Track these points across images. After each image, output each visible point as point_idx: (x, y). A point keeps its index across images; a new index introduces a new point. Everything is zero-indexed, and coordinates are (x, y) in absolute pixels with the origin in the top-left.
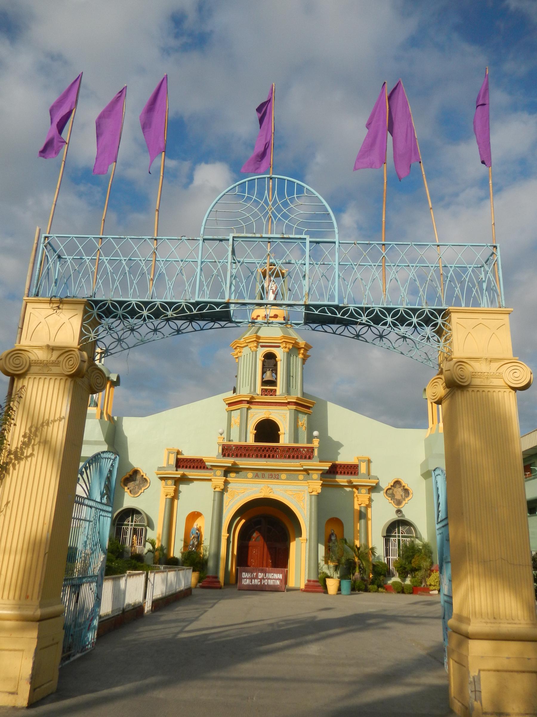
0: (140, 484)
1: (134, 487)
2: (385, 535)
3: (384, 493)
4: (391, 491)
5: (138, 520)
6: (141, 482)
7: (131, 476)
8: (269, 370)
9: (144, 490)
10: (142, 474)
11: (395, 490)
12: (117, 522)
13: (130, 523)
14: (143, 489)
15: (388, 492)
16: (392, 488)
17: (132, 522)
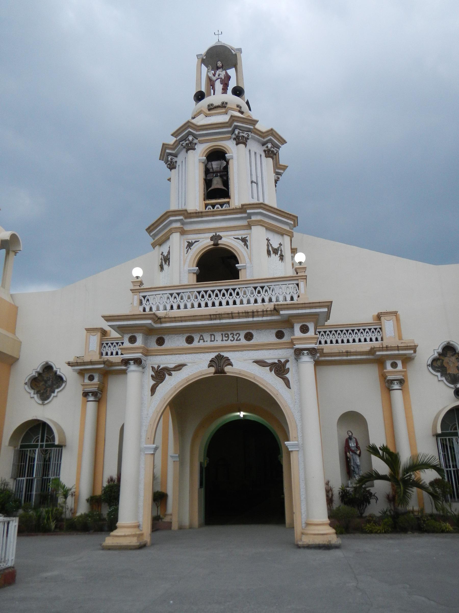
1: (45, 389)
2: (439, 431)
3: (428, 365)
4: (439, 363)
5: (51, 437)
6: (54, 382)
7: (39, 374)
8: (216, 176)
9: (58, 392)
10: (55, 369)
11: (446, 359)
12: (21, 443)
13: (39, 443)
14: (57, 391)
15: (435, 364)
16: (442, 357)
17: (42, 441)
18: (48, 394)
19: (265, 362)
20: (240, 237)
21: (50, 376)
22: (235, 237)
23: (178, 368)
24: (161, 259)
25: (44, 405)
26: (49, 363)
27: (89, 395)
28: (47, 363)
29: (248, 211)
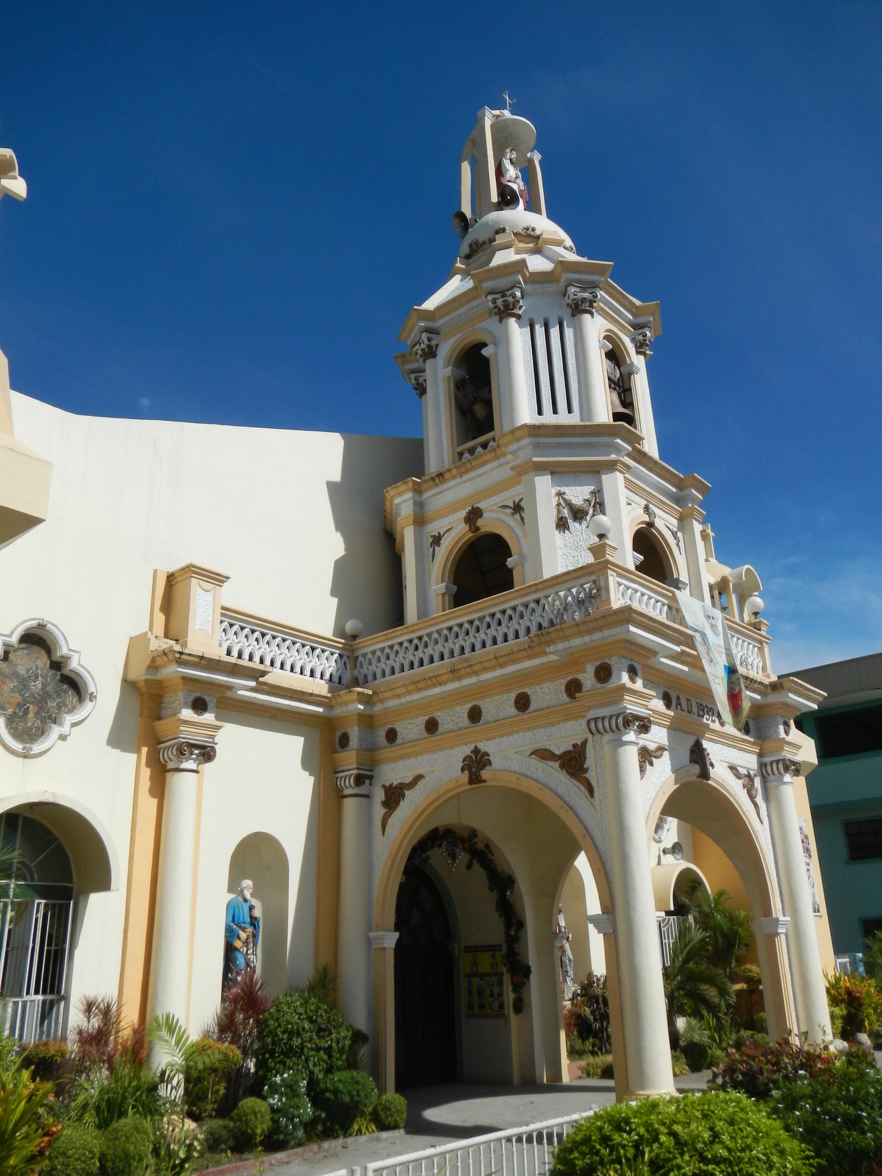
0: (41, 701)
1: (19, 705)
5: (32, 865)
9: (74, 725)
14: (69, 719)
18: (30, 724)
19: (737, 770)
20: (671, 527)
21: (37, 669)
22: (668, 525)
23: (659, 752)
24: (559, 505)
25: (25, 757)
26: (48, 625)
27: (192, 753)
28: (41, 626)
29: (693, 491)
